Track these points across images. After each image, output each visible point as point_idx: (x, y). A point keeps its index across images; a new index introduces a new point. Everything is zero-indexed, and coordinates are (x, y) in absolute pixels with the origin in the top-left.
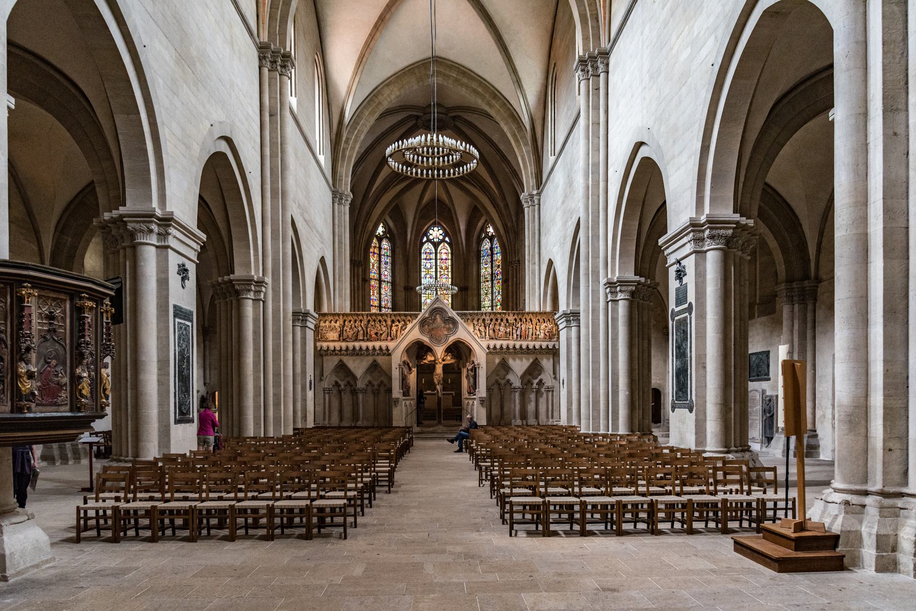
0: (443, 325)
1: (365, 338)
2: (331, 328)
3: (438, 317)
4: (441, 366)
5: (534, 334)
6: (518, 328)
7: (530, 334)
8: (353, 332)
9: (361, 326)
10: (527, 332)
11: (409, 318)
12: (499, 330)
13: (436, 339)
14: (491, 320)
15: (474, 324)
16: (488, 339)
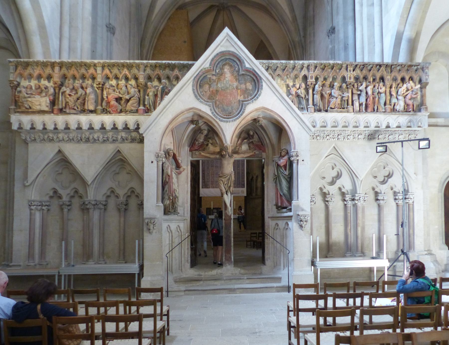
0: (235, 84)
1: (99, 107)
2: (39, 90)
3: (227, 69)
4: (232, 161)
5: (388, 102)
6: (361, 91)
7: (382, 102)
8: (75, 97)
9: (92, 86)
10: (377, 99)
11: (176, 72)
12: (330, 95)
13: (223, 110)
14: (317, 79)
15: (288, 86)
16: (313, 110)
